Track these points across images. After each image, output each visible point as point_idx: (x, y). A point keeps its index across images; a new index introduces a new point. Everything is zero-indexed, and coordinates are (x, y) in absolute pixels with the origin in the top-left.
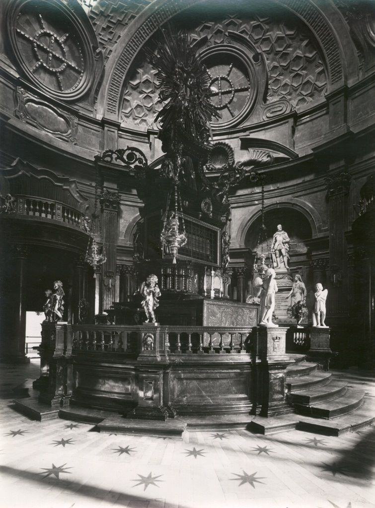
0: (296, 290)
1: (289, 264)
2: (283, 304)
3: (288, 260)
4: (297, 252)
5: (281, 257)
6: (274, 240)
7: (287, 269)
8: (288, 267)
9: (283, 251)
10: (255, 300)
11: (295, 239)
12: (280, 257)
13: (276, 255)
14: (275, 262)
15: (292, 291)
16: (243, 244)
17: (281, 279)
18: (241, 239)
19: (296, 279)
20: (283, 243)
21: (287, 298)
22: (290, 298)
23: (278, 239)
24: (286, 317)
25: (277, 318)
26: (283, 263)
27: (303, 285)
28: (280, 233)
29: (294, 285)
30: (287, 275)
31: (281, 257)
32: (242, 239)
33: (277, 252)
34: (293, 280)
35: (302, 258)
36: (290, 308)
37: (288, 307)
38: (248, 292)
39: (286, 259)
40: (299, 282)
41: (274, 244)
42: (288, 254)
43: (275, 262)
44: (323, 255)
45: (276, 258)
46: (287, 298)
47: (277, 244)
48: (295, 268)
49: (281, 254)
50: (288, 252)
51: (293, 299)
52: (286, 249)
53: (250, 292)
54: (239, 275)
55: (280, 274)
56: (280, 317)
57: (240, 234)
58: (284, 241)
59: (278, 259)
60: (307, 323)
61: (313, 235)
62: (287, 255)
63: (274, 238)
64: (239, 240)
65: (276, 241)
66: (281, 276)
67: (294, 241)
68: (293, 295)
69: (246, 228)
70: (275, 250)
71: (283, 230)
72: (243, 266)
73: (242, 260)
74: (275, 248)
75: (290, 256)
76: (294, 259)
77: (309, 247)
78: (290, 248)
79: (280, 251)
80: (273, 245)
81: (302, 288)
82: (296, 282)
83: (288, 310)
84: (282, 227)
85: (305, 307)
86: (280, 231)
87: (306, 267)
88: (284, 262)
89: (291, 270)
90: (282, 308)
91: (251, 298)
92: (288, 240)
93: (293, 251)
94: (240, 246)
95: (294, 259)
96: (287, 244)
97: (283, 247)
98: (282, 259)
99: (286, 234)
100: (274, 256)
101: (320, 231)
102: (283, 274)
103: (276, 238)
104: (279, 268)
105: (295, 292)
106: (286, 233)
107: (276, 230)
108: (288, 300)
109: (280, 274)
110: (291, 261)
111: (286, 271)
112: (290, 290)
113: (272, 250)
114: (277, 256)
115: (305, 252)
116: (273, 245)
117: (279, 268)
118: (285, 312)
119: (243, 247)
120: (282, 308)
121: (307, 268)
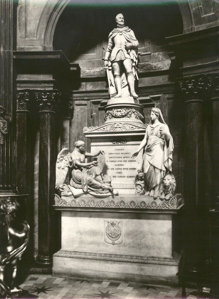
0: (153, 139)
1: (137, 89)
2: (128, 165)
3: (136, 82)
4: (151, 68)
5: (124, 75)
6: (110, 44)
7: (135, 98)
8: (136, 95)
9: (128, 64)
10: (74, 158)
11: (148, 45)
12: (121, 75)
13: (113, 72)
14: (112, 85)
15: (144, 141)
16: (51, 46)
17: (123, 116)
18: (45, 35)
19: (153, 116)
20: (127, 49)
21: (136, 154)
22: (141, 154)
23: (117, 40)
24: (133, 192)
25: (117, 195)
26: (127, 87)
27: (166, 129)
28: (120, 30)
29: (149, 129)
30: (134, 110)
31: (124, 75)
32: (48, 35)
33: (116, 65)
34: (145, 120)
35: (161, 80)
36: (141, 174)
37: (135, 173)
38: (63, 141)
39: (131, 80)
40: (157, 122)
41: (111, 51)
42: (136, 70)
43: (112, 85)
44: (210, 69)
45: (115, 76)
46: (136, 154)
47: (115, 51)
48: (148, 98)
49: (123, 70)
50: (136, 67)
51: (147, 157)
52: (132, 60)
53: (68, 142)
54: (43, 108)
55: (121, 107)
56: (121, 192)
57: (45, 26)
58: (129, 45)
59: (118, 79)
60: (175, 207)
61: (185, 29)
62: (135, 73)
63: (110, 40)
64: (43, 36)
65: (113, 46)
66: (124, 111)
67: (146, 48)
68: (147, 150)
69: (56, 13)
70: (112, 62)
71: (126, 25)
72: (52, 89)
73: (49, 78)
74: (112, 59)
75: (140, 75)
76: (147, 81)
77: (174, 58)
78: (138, 59)
79: (121, 63)
80: (107, 54)
81: (166, 136)
82: (153, 122)
83: (138, 178)
84: (124, 18)
85: (170, 173)
86: (121, 26)
87: (167, 96)
88: (128, 85)
89: (141, 101)
90: (125, 173)
91: (66, 152)
92: (136, 43)
93: (143, 66)
94: (45, 48)
95: (147, 81)
96: (133, 52)
97: (127, 56)
98: (125, 81)
99: (132, 33)
100: (110, 74)
101: (200, 21)
102: (127, 107)
103: (113, 39)
104: (120, 97)
105: (150, 142)
106: (132, 32)
107: (115, 25)
108: (136, 158)
109: (121, 107)
110: (140, 85)
111: (133, 102)
112: (141, 138)
113: (106, 62)
114: (117, 73)
115: (167, 68)
116: (107, 54)
117: (120, 97)
118: (131, 181)
119: (50, 47)
120: (125, 173)
121: (168, 99)
